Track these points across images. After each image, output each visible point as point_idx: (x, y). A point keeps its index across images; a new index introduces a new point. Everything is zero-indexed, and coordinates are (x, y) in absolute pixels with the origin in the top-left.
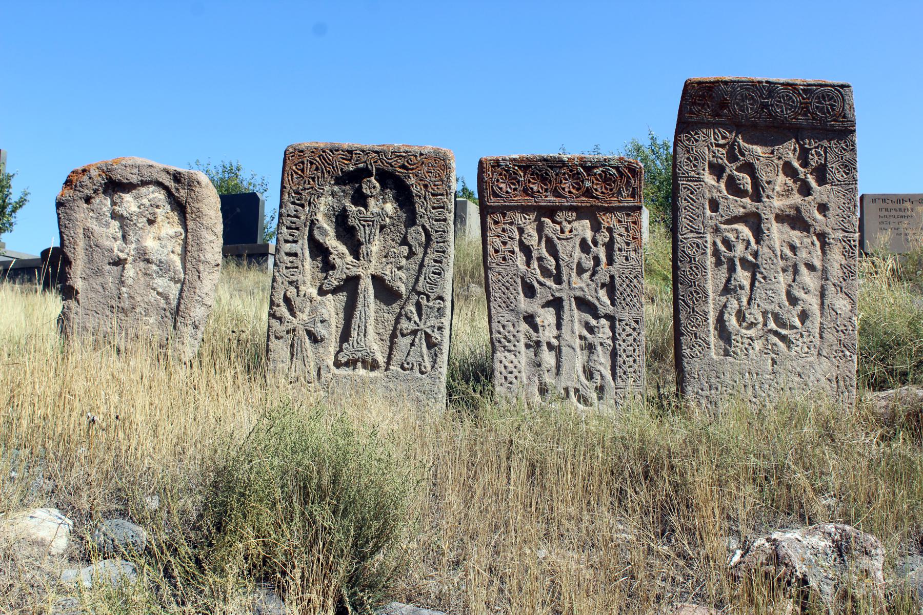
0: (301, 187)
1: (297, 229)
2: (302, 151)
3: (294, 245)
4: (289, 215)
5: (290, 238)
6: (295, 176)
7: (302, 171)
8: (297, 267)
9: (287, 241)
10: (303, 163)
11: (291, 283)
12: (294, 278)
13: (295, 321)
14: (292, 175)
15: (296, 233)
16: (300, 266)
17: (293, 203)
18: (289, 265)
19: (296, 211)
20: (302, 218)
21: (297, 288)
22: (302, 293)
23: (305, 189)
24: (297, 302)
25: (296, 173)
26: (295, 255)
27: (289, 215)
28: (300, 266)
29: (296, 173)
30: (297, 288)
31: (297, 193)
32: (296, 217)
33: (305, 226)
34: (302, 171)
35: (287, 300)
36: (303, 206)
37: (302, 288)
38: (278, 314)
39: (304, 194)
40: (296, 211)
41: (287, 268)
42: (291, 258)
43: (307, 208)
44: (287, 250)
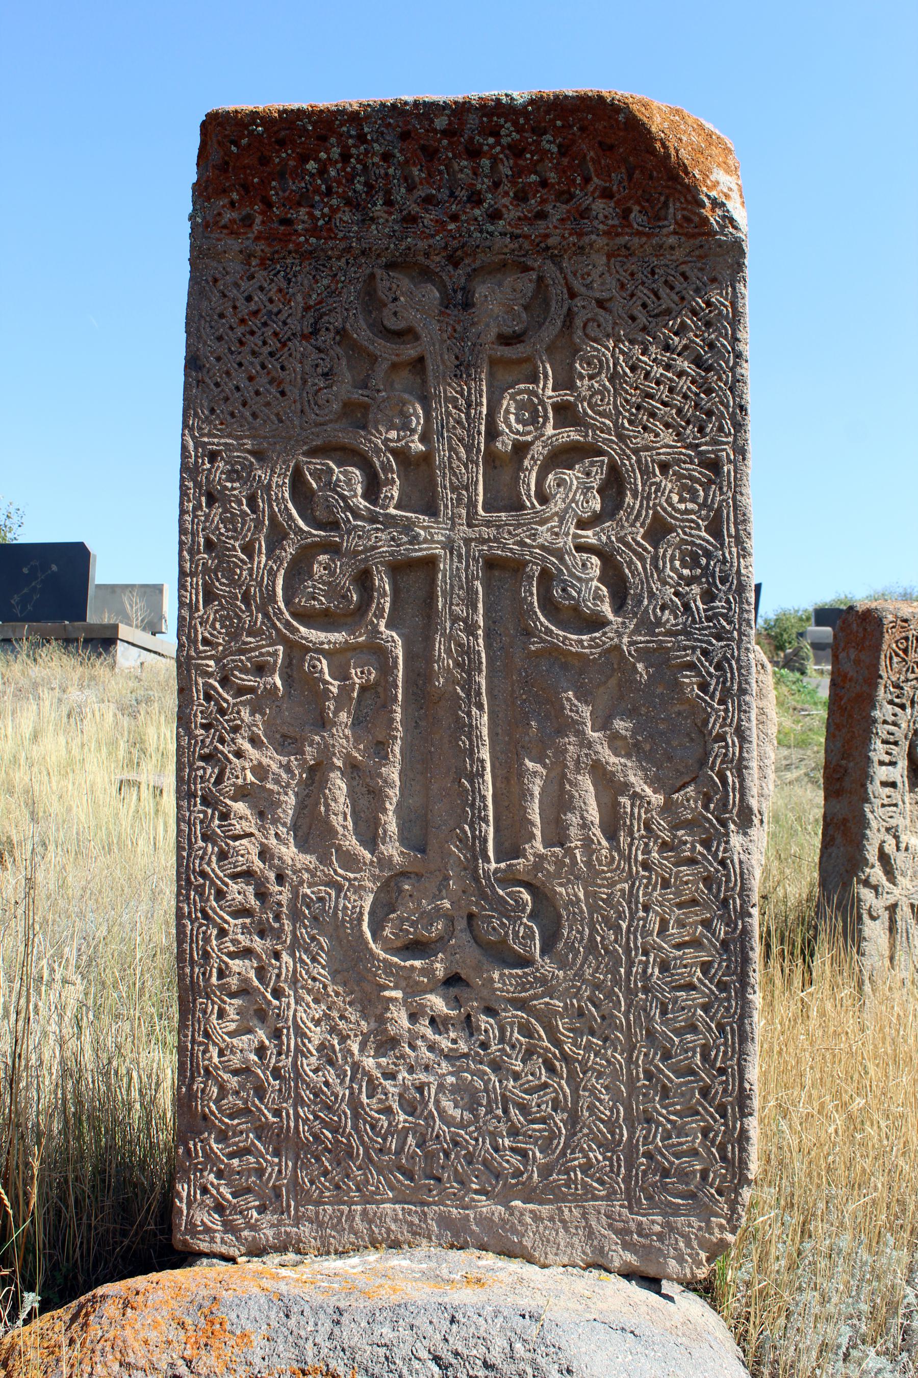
0: (902, 678)
1: (896, 743)
2: (906, 621)
3: (890, 768)
4: (885, 722)
5: (887, 758)
6: (895, 659)
7: (905, 651)
8: (896, 805)
9: (882, 763)
10: (907, 639)
11: (888, 830)
12: (893, 822)
13: (896, 891)
14: (891, 658)
15: (895, 750)
16: (900, 803)
17: (891, 702)
18: (886, 802)
19: (895, 715)
20: (904, 725)
21: (896, 837)
22: (903, 846)
23: (907, 680)
24: (900, 860)
25: (897, 655)
26: (893, 785)
27: (885, 722)
28: (900, 803)
29: (897, 655)
30: (896, 837)
31: (897, 686)
32: (895, 724)
33: (906, 738)
34: (905, 651)
35: (884, 858)
36: (903, 707)
37: (904, 838)
38: (873, 881)
39: (907, 687)
40: (895, 715)
41: (883, 806)
42: (888, 791)
43: (909, 710)
44: (884, 779)
